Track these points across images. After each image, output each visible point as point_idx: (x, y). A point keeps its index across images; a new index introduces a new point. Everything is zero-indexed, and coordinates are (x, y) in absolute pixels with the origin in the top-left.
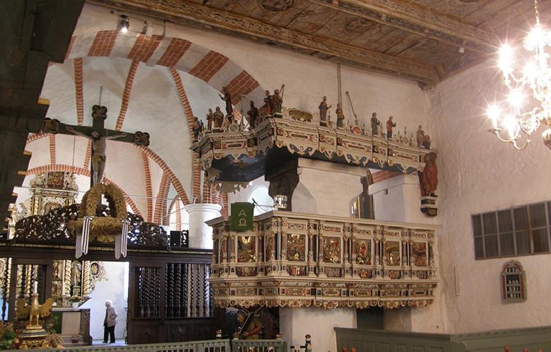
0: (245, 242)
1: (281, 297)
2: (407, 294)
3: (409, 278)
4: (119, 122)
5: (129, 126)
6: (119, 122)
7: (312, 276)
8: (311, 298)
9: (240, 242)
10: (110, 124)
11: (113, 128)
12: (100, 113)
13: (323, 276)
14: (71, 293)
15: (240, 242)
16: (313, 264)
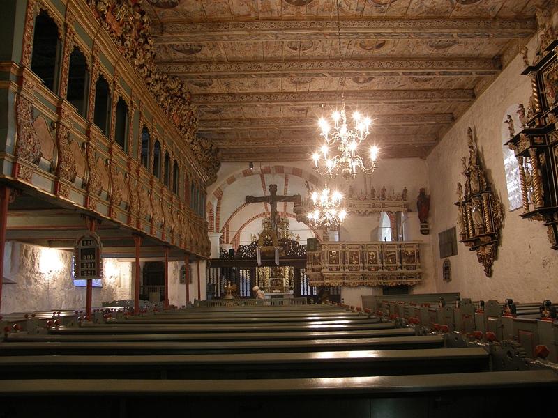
0: (317, 256)
1: (326, 282)
2: (402, 278)
3: (401, 270)
4: (285, 191)
5: (290, 193)
6: (285, 191)
7: (342, 270)
8: (342, 281)
9: (314, 256)
10: (280, 192)
11: (282, 194)
12: (273, 188)
13: (347, 271)
14: (290, 284)
15: (314, 256)
16: (342, 265)
